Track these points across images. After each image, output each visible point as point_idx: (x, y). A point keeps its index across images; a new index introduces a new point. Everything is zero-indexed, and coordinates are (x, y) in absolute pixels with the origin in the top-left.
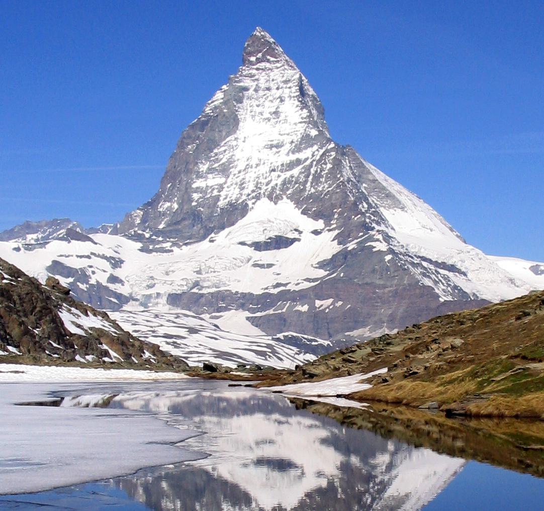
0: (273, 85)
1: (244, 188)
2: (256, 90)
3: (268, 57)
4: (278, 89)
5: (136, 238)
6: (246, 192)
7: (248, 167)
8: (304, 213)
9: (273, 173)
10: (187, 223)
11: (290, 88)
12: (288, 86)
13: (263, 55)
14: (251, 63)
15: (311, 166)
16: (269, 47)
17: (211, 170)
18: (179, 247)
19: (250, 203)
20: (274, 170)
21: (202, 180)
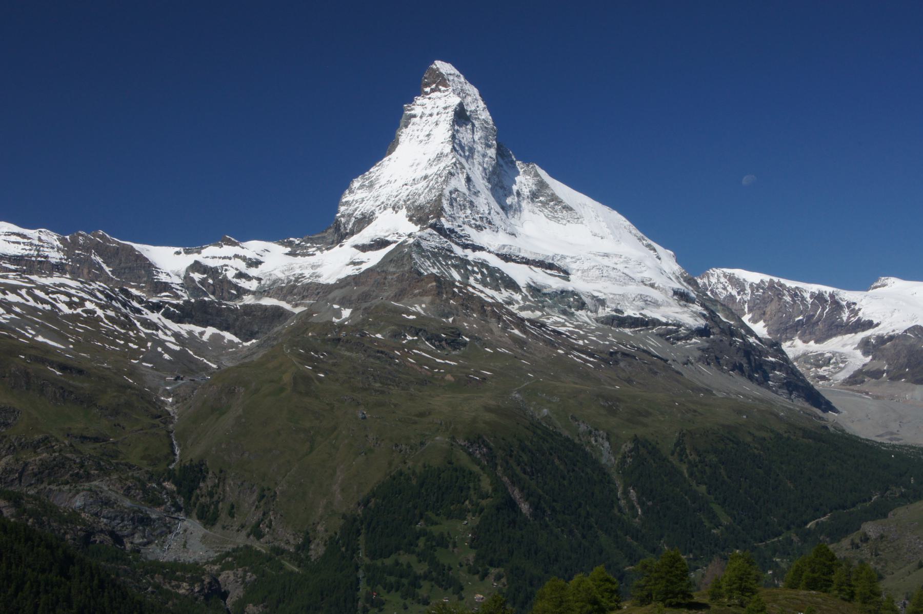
2: (421, 117)
4: (438, 114)
7: (389, 182)
8: (410, 220)
13: (437, 86)
14: (427, 93)
17: (362, 187)
18: (322, 251)
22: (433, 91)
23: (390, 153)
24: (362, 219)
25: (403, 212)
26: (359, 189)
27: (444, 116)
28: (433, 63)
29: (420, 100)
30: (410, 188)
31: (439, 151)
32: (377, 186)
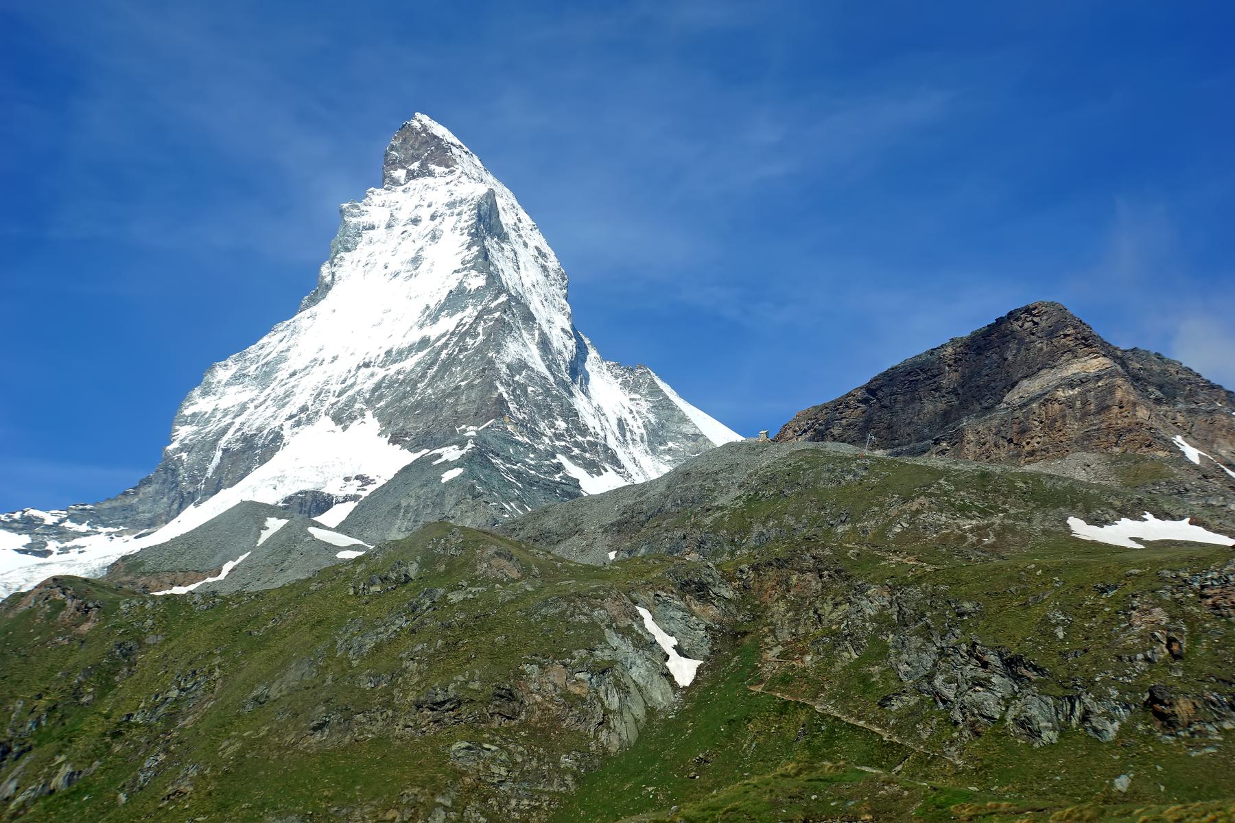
0: (425, 214)
1: (284, 406)
2: (389, 226)
3: (432, 167)
4: (433, 217)
5: (21, 526)
6: (287, 411)
9: (363, 370)
10: (150, 489)
11: (459, 214)
12: (456, 211)
13: (423, 165)
14: (396, 182)
15: (446, 345)
16: (437, 148)
17: (238, 378)
19: (286, 432)
20: (367, 365)
21: (214, 398)
22: (411, 175)
23: (314, 301)
24: (243, 451)
25: (371, 424)
26: (228, 384)
27: (450, 222)
28: (413, 117)
29: (378, 196)
30: (381, 373)
31: (453, 284)
32: (282, 374)
